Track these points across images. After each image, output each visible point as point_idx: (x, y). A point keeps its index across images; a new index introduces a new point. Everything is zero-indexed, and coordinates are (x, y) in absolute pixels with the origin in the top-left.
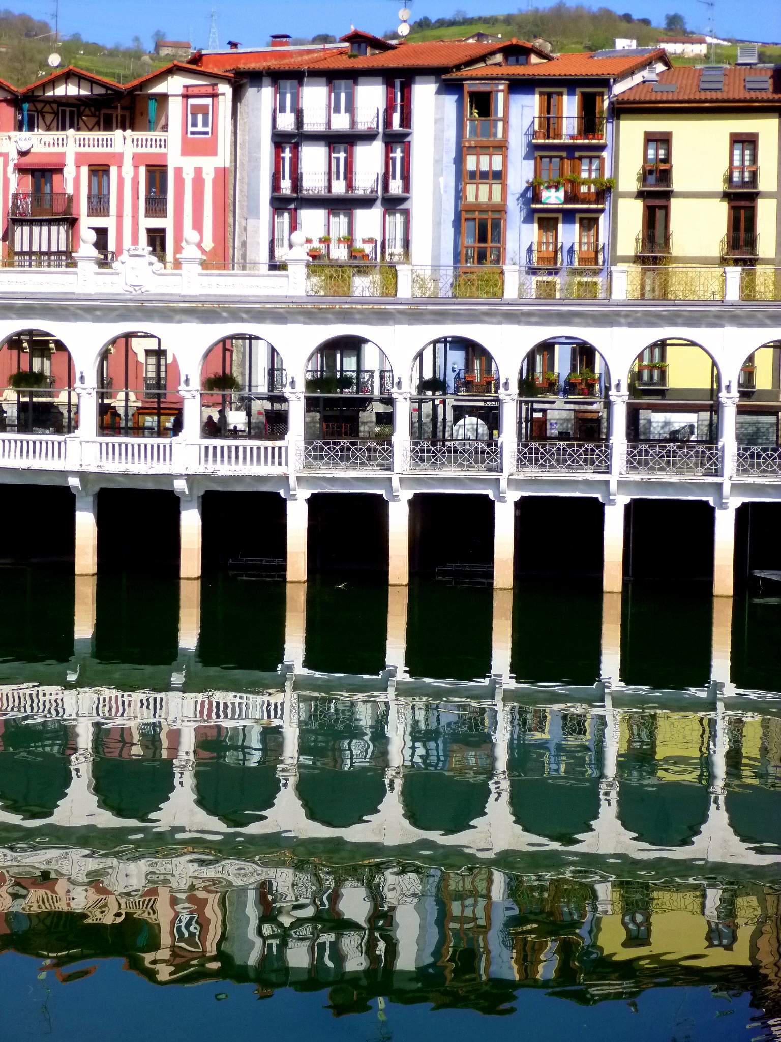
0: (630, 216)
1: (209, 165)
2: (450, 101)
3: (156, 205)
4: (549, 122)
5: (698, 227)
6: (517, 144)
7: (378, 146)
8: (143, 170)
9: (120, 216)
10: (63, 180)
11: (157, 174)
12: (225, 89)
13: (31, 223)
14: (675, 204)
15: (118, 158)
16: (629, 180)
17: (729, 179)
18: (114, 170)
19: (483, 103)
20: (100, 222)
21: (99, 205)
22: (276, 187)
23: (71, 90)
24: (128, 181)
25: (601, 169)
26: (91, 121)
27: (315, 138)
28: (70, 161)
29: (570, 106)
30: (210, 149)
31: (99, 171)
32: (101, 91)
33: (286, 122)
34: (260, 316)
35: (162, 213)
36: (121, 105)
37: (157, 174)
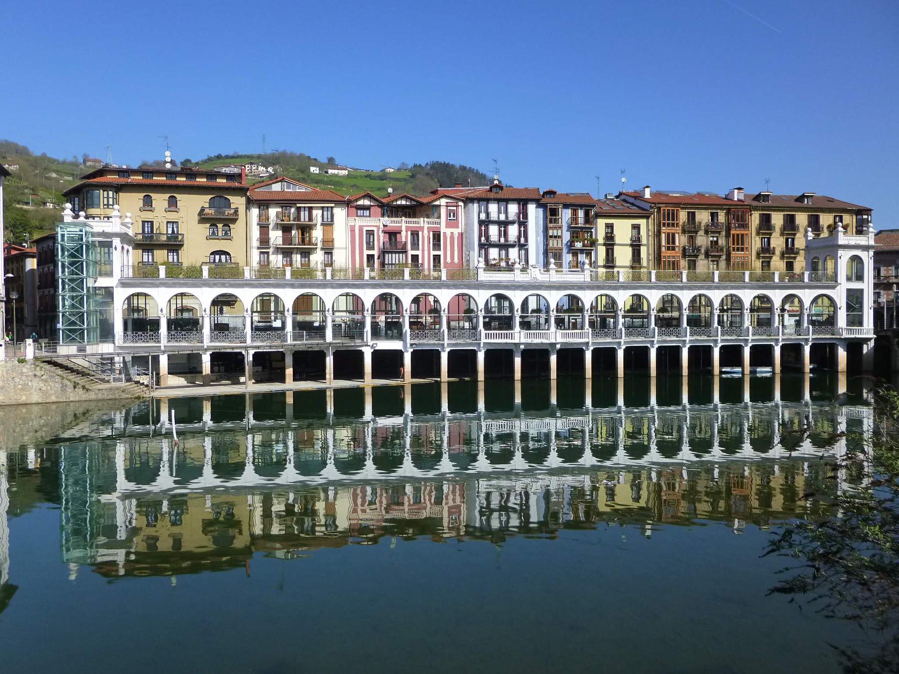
0: (602, 251)
2: (541, 211)
3: (437, 246)
4: (575, 218)
5: (623, 256)
6: (565, 228)
7: (516, 226)
8: (431, 233)
9: (423, 250)
11: (437, 236)
13: (392, 253)
15: (422, 228)
16: (601, 240)
17: (631, 240)
18: (420, 233)
19: (554, 212)
20: (415, 253)
21: (415, 245)
22: (480, 240)
23: (404, 202)
24: (425, 236)
25: (591, 236)
27: (494, 222)
28: (404, 229)
29: (581, 213)
31: (415, 234)
32: (414, 203)
33: (483, 216)
34: (507, 287)
35: (373, 249)
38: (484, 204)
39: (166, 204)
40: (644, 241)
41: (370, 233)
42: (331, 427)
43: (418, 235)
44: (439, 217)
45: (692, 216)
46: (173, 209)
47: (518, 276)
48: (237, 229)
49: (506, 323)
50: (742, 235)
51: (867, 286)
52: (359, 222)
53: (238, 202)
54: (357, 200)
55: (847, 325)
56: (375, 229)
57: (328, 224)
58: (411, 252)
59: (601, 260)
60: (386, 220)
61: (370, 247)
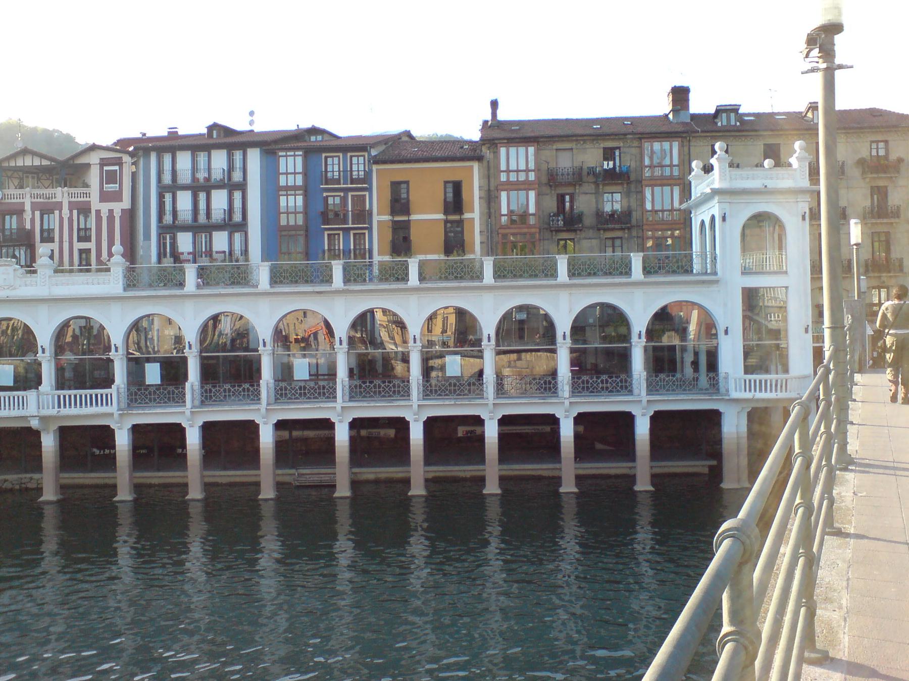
9: (61, 242)
15: (59, 206)
23: (28, 161)
28: (28, 207)
30: (117, 197)
32: (45, 163)
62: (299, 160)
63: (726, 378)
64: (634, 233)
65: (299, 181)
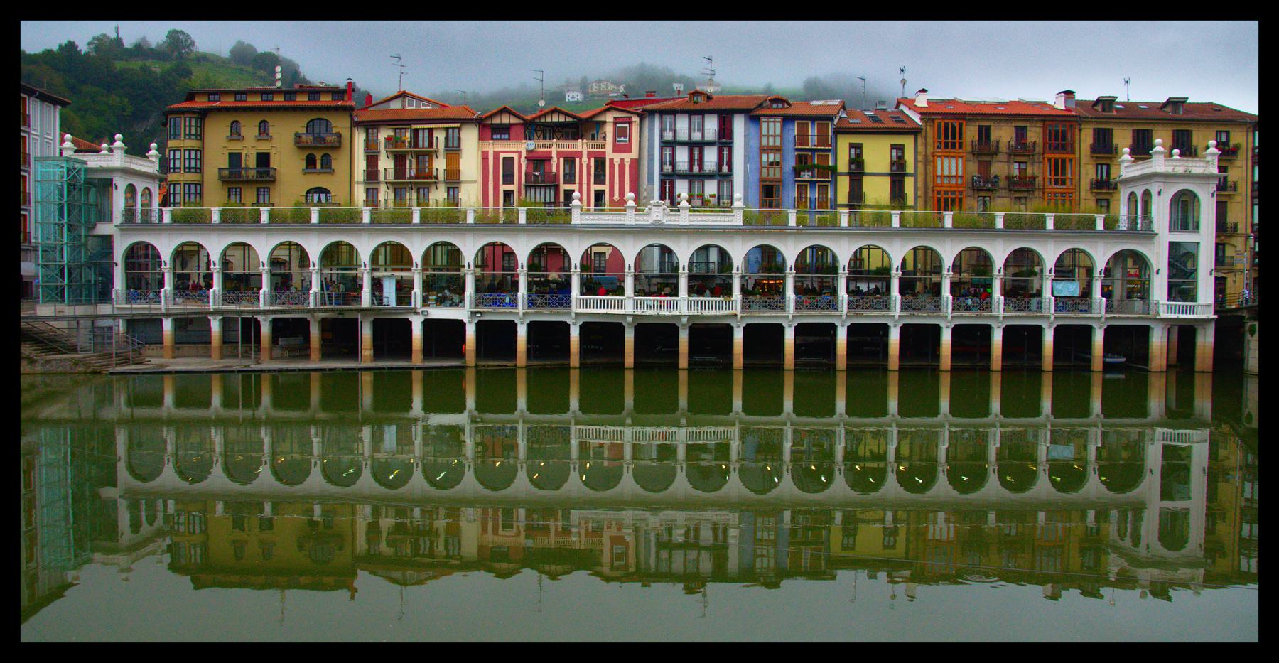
0: (844, 184)
1: (627, 158)
3: (600, 179)
4: (802, 138)
5: (877, 190)
10: (550, 165)
12: (636, 119)
14: (866, 180)
15: (580, 154)
16: (843, 166)
18: (577, 160)
20: (569, 187)
21: (570, 178)
22: (661, 169)
23: (555, 119)
24: (584, 165)
26: (559, 135)
27: (683, 144)
28: (554, 155)
29: (813, 131)
30: (628, 149)
31: (570, 160)
32: (568, 119)
33: (668, 136)
36: (579, 127)
37: (600, 162)
38: (668, 119)
39: (256, 132)
40: (910, 168)
41: (509, 162)
42: (366, 421)
43: (574, 162)
44: (604, 138)
45: (984, 133)
46: (265, 137)
47: (629, 219)
48: (339, 163)
49: (665, 285)
50: (1063, 161)
51: (1205, 239)
52: (492, 147)
53: (340, 124)
54: (491, 116)
55: (1169, 298)
56: (515, 156)
57: (454, 151)
58: (564, 187)
59: (843, 197)
60: (531, 145)
61: (508, 178)
62: (778, 125)
63: (1157, 304)
64: (1036, 194)
65: (778, 143)
